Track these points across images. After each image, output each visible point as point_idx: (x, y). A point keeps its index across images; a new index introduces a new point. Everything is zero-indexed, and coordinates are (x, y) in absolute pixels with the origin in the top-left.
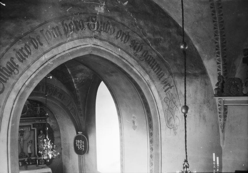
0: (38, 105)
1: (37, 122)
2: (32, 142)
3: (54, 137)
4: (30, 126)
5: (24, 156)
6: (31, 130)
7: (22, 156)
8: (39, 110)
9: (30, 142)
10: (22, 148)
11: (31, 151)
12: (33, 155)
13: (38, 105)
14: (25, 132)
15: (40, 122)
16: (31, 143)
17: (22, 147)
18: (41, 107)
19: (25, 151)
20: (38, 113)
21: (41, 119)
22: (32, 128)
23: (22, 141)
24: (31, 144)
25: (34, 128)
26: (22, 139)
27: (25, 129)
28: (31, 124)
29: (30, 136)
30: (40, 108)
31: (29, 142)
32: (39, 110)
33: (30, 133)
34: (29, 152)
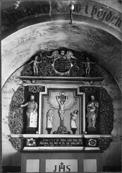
0: (88, 59)
1: (87, 84)
2: (78, 113)
3: (114, 108)
4: (76, 90)
5: (65, 131)
6: (77, 95)
7: (62, 131)
8: (89, 66)
9: (76, 112)
10: (62, 120)
11: (76, 126)
12: (77, 132)
13: (88, 59)
14: (67, 97)
15: (91, 84)
16: (77, 113)
17: (62, 118)
18: (92, 63)
19: (66, 124)
20: (88, 71)
21: (94, 81)
22: (79, 93)
23: (62, 109)
24: (75, 115)
25: (82, 93)
26: (62, 107)
27: (66, 94)
28: (75, 86)
29: (75, 104)
30: (90, 64)
31: (74, 112)
32: (89, 66)
33: (76, 100)
34: (74, 126)
